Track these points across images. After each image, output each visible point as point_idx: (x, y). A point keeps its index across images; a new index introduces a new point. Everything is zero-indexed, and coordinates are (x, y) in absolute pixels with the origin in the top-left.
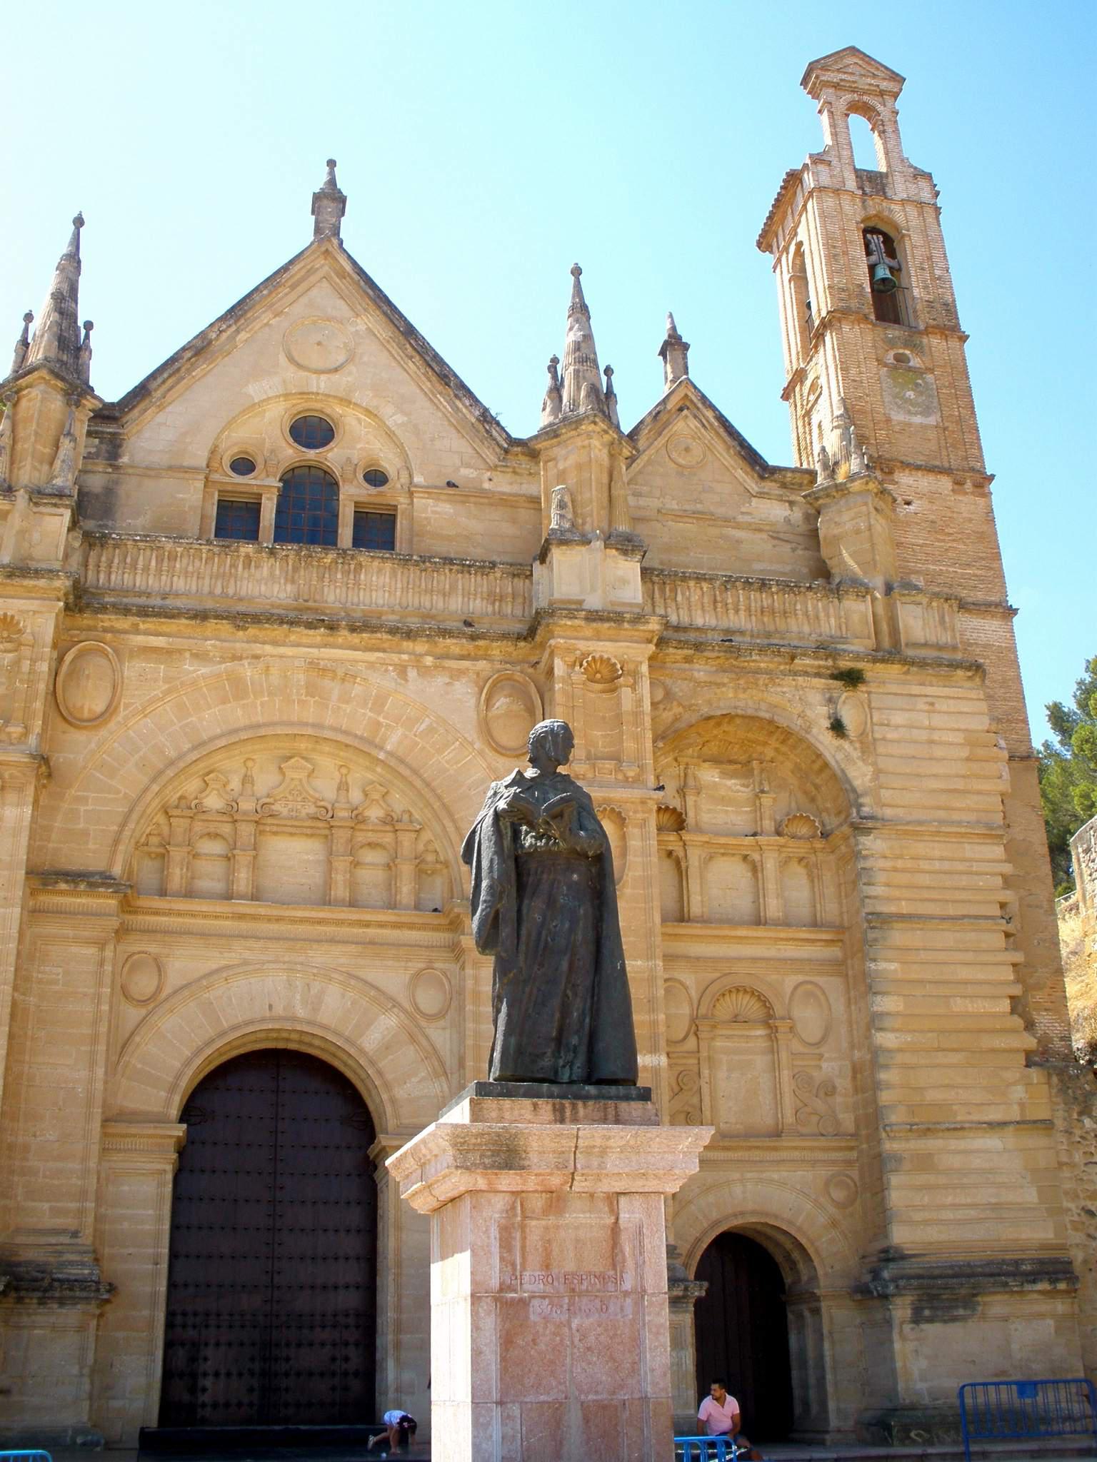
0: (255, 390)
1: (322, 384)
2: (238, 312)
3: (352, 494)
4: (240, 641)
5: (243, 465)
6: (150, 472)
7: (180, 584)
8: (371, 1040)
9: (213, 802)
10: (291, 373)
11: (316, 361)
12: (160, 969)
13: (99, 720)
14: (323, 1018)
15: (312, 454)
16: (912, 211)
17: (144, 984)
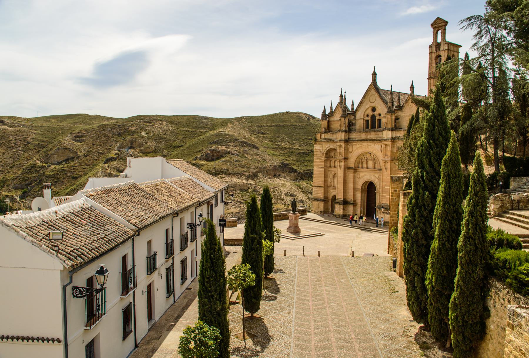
0: (367, 107)
1: (373, 105)
2: (364, 97)
3: (377, 118)
4: (361, 143)
5: (368, 116)
6: (358, 120)
7: (357, 137)
8: (375, 182)
9: (363, 158)
10: (370, 103)
11: (372, 101)
12: (360, 174)
13: (351, 152)
14: (372, 180)
15: (373, 113)
16: (443, 52)
17: (358, 176)
